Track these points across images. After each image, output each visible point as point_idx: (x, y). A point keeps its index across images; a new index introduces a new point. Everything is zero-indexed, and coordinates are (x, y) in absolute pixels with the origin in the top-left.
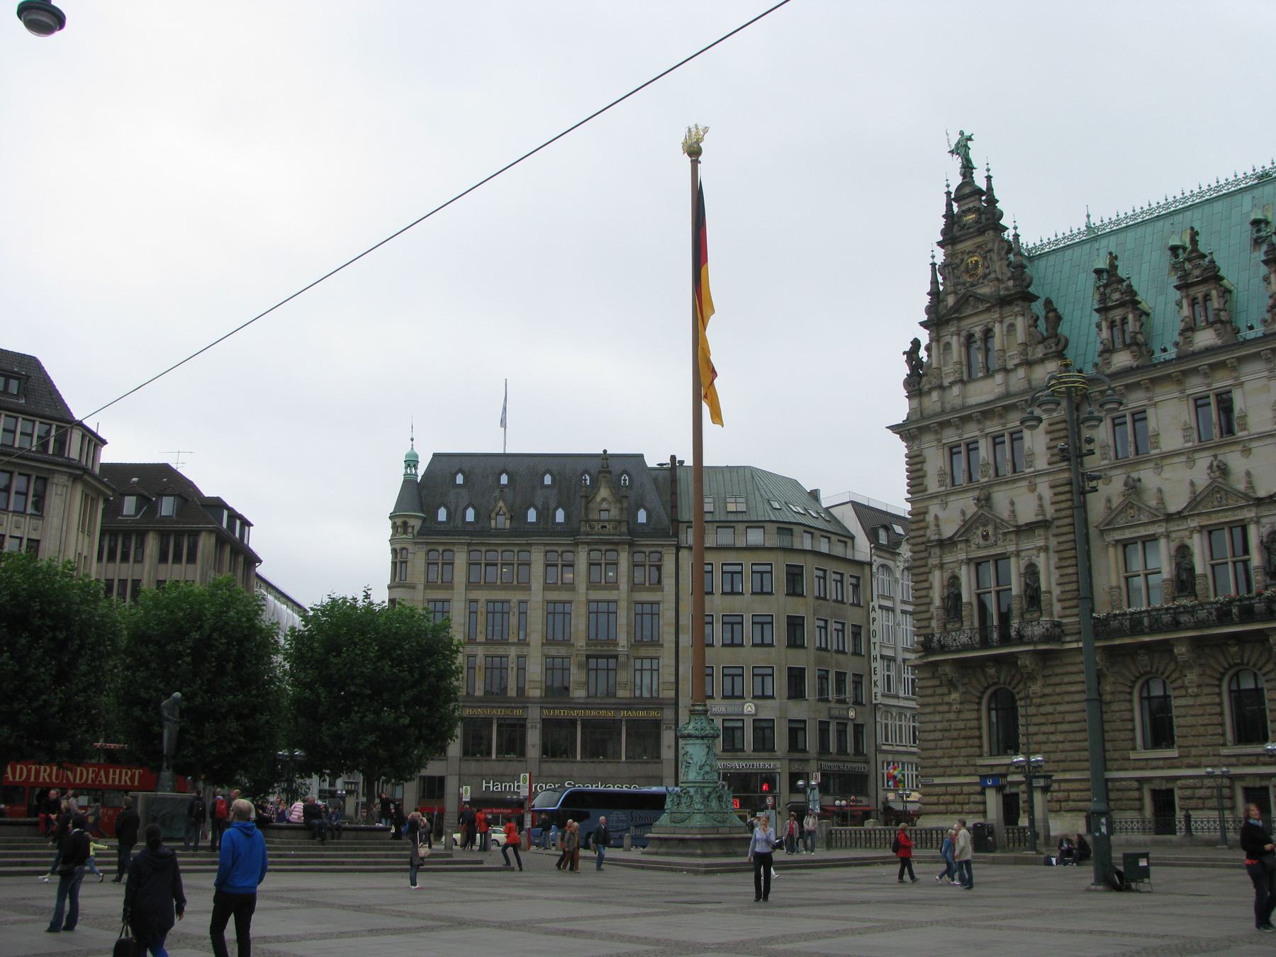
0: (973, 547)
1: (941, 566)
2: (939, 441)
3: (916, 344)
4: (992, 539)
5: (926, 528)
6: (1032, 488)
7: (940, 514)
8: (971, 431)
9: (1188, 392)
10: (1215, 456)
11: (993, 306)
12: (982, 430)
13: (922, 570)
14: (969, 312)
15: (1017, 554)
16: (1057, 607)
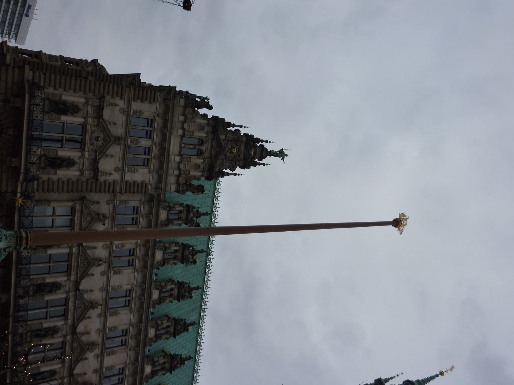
0: (93, 129)
1: (86, 103)
2: (158, 116)
3: (211, 108)
4: (95, 142)
5: (112, 97)
6: (116, 169)
7: (117, 108)
8: (157, 137)
9: (138, 248)
10: (105, 262)
11: (212, 161)
12: (155, 143)
13: (88, 88)
14: (214, 145)
15: (82, 157)
16: (45, 177)
